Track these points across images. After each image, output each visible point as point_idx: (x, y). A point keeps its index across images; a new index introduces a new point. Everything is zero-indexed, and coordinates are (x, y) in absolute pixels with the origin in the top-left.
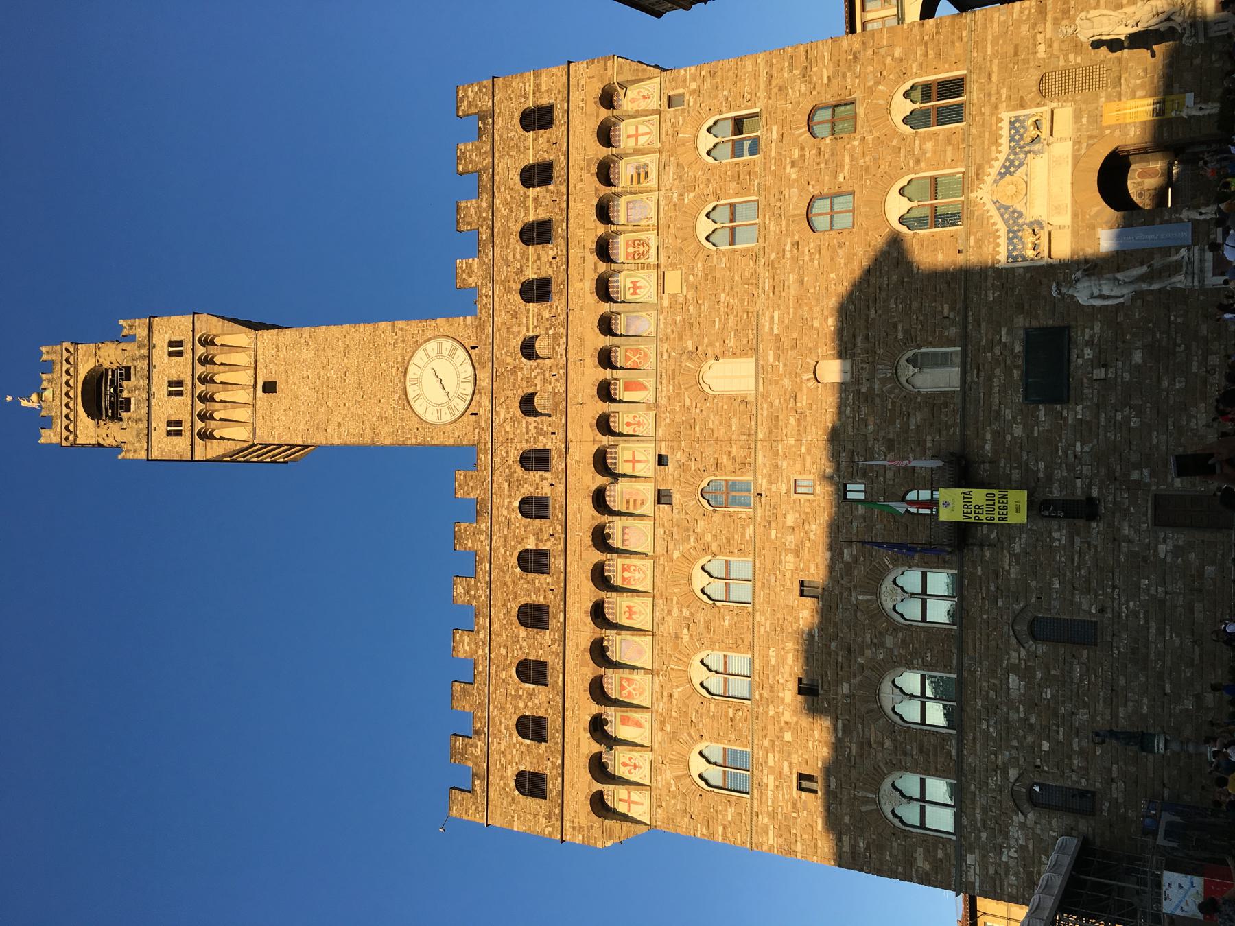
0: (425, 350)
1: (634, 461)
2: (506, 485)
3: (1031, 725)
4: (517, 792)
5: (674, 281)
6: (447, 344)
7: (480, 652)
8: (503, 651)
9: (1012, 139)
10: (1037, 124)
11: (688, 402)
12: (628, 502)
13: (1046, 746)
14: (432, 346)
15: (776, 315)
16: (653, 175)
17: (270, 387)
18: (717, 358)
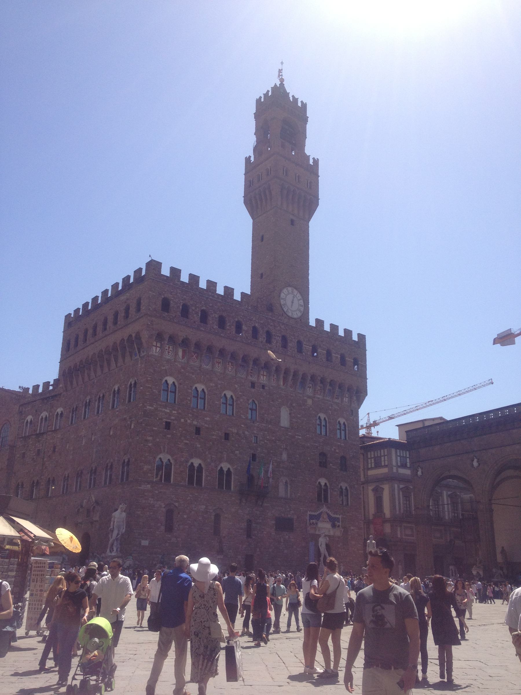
0: (301, 299)
1: (263, 375)
2: (262, 322)
3: (191, 512)
4: (163, 297)
5: (310, 402)
6: (302, 309)
7: (210, 294)
8: (211, 305)
9: (335, 518)
10: (339, 526)
11: (280, 400)
12: (252, 370)
13: (185, 516)
14: (301, 302)
15: (300, 437)
16: (336, 401)
17: (292, 222)
18: (290, 414)
